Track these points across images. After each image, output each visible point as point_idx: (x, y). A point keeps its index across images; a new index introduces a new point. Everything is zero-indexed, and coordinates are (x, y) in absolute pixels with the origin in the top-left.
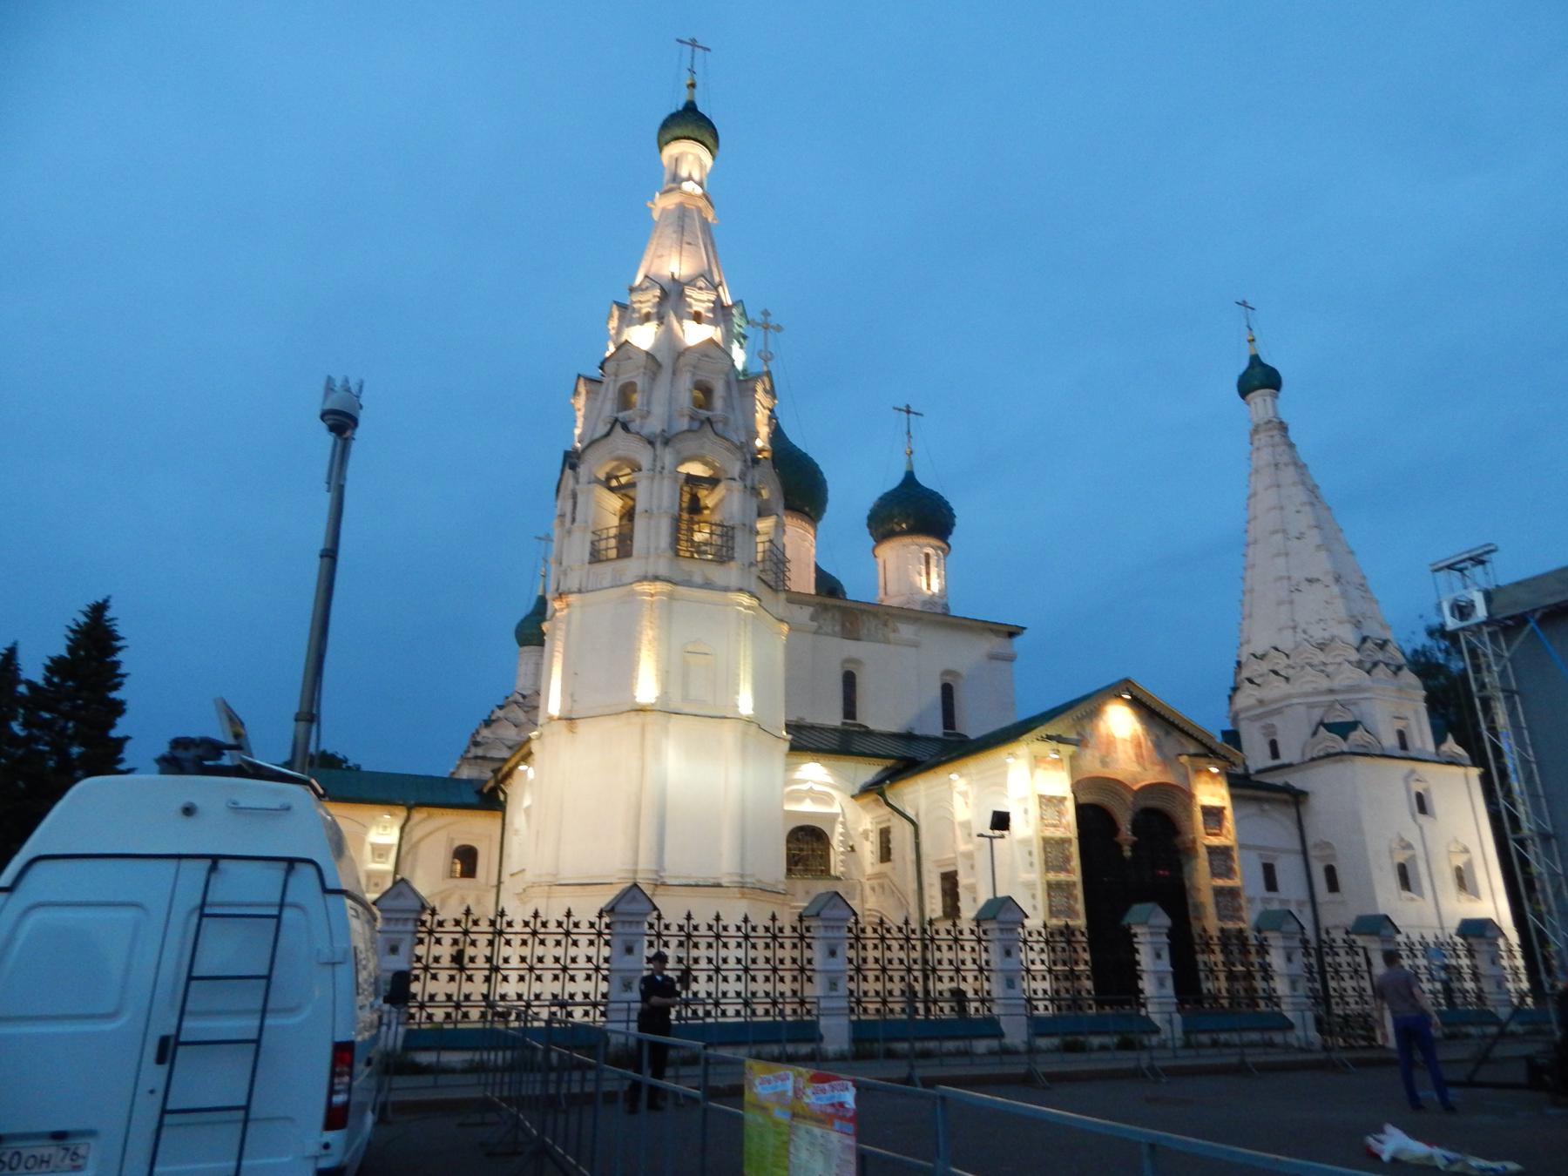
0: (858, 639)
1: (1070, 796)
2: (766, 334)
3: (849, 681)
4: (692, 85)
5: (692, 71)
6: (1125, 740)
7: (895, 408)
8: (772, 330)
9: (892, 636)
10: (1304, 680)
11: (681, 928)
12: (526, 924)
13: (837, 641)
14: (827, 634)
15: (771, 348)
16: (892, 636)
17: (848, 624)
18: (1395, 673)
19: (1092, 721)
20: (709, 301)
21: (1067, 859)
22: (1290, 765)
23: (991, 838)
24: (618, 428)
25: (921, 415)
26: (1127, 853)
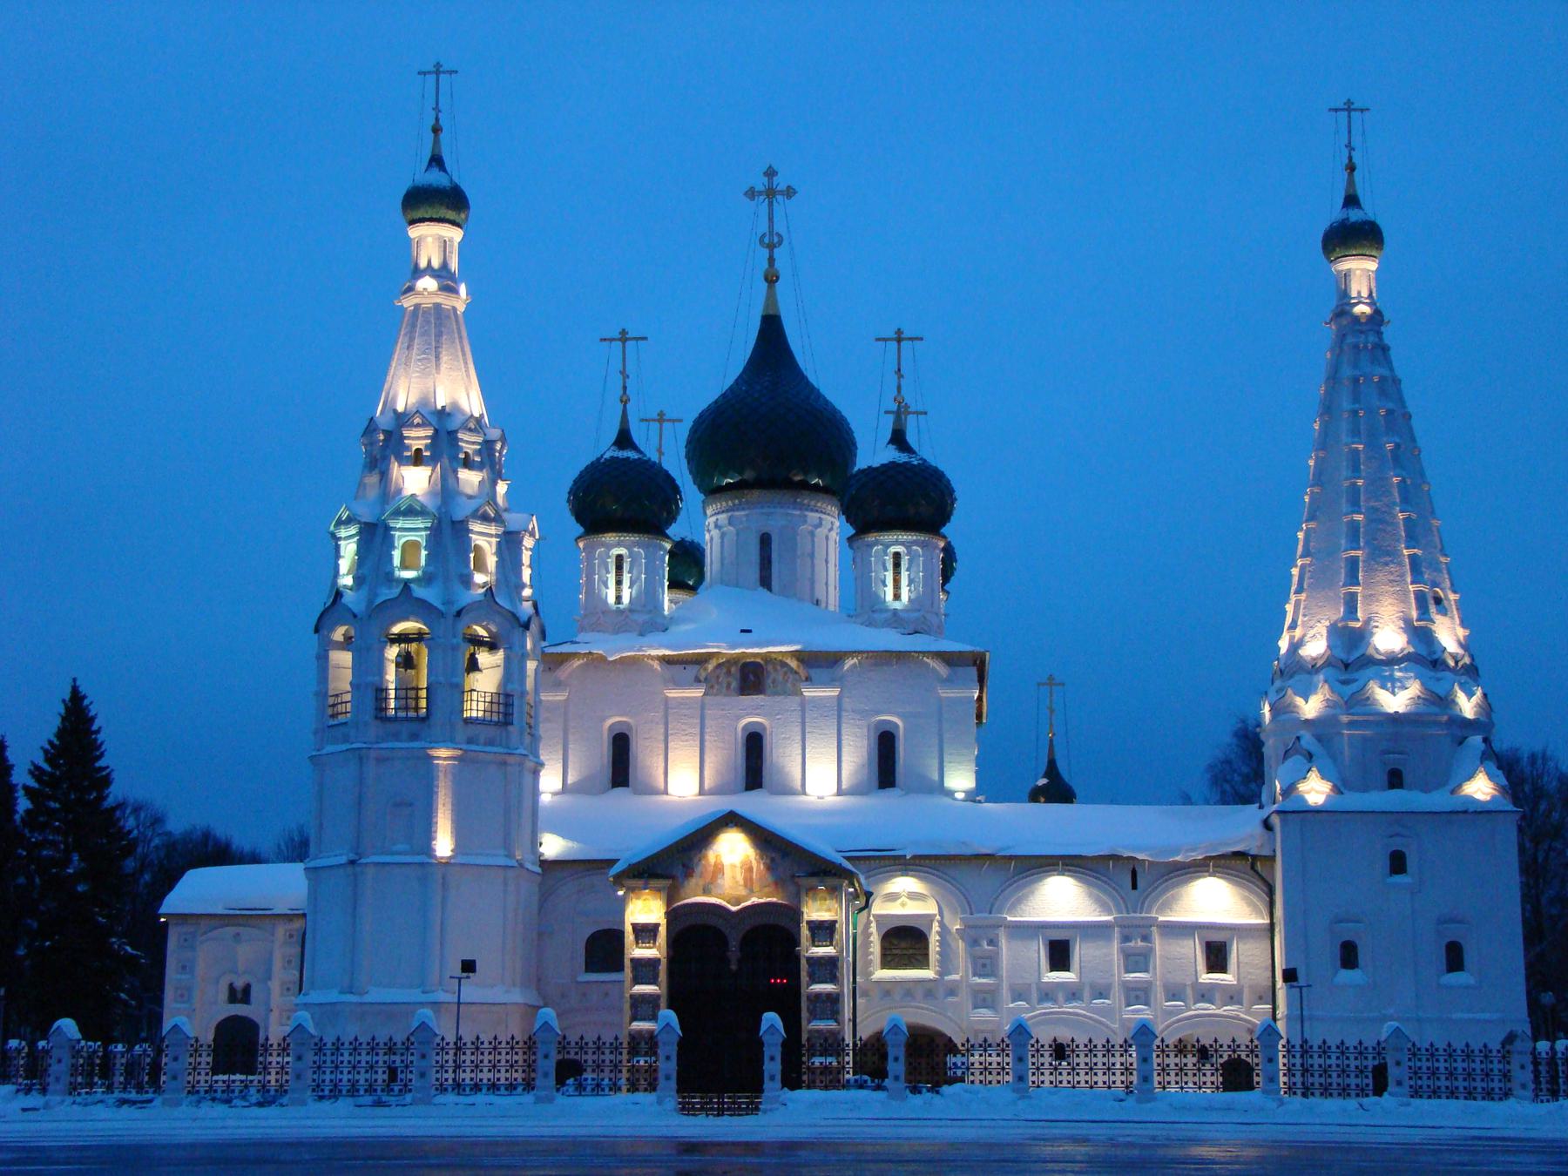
1: (663, 922)
2: (771, 204)
4: (436, 130)
5: (437, 109)
6: (734, 866)
7: (878, 340)
8: (779, 198)
15: (779, 227)
19: (701, 851)
20: (426, 437)
23: (460, 979)
25: (922, 339)
26: (734, 967)
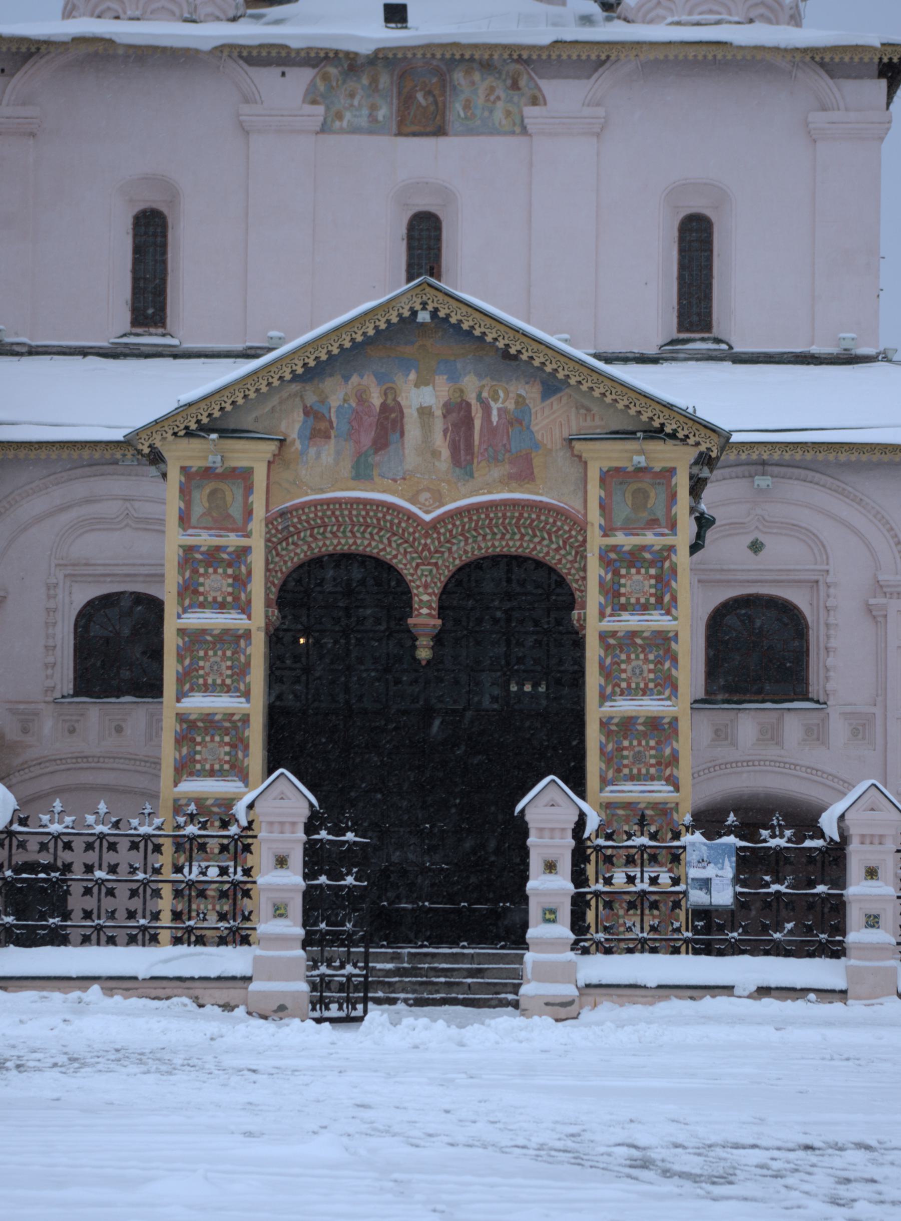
0: (440, 131)
6: (425, 412)
9: (530, 111)
13: (385, 141)
14: (355, 130)
17: (420, 96)
21: (242, 671)
26: (424, 654)
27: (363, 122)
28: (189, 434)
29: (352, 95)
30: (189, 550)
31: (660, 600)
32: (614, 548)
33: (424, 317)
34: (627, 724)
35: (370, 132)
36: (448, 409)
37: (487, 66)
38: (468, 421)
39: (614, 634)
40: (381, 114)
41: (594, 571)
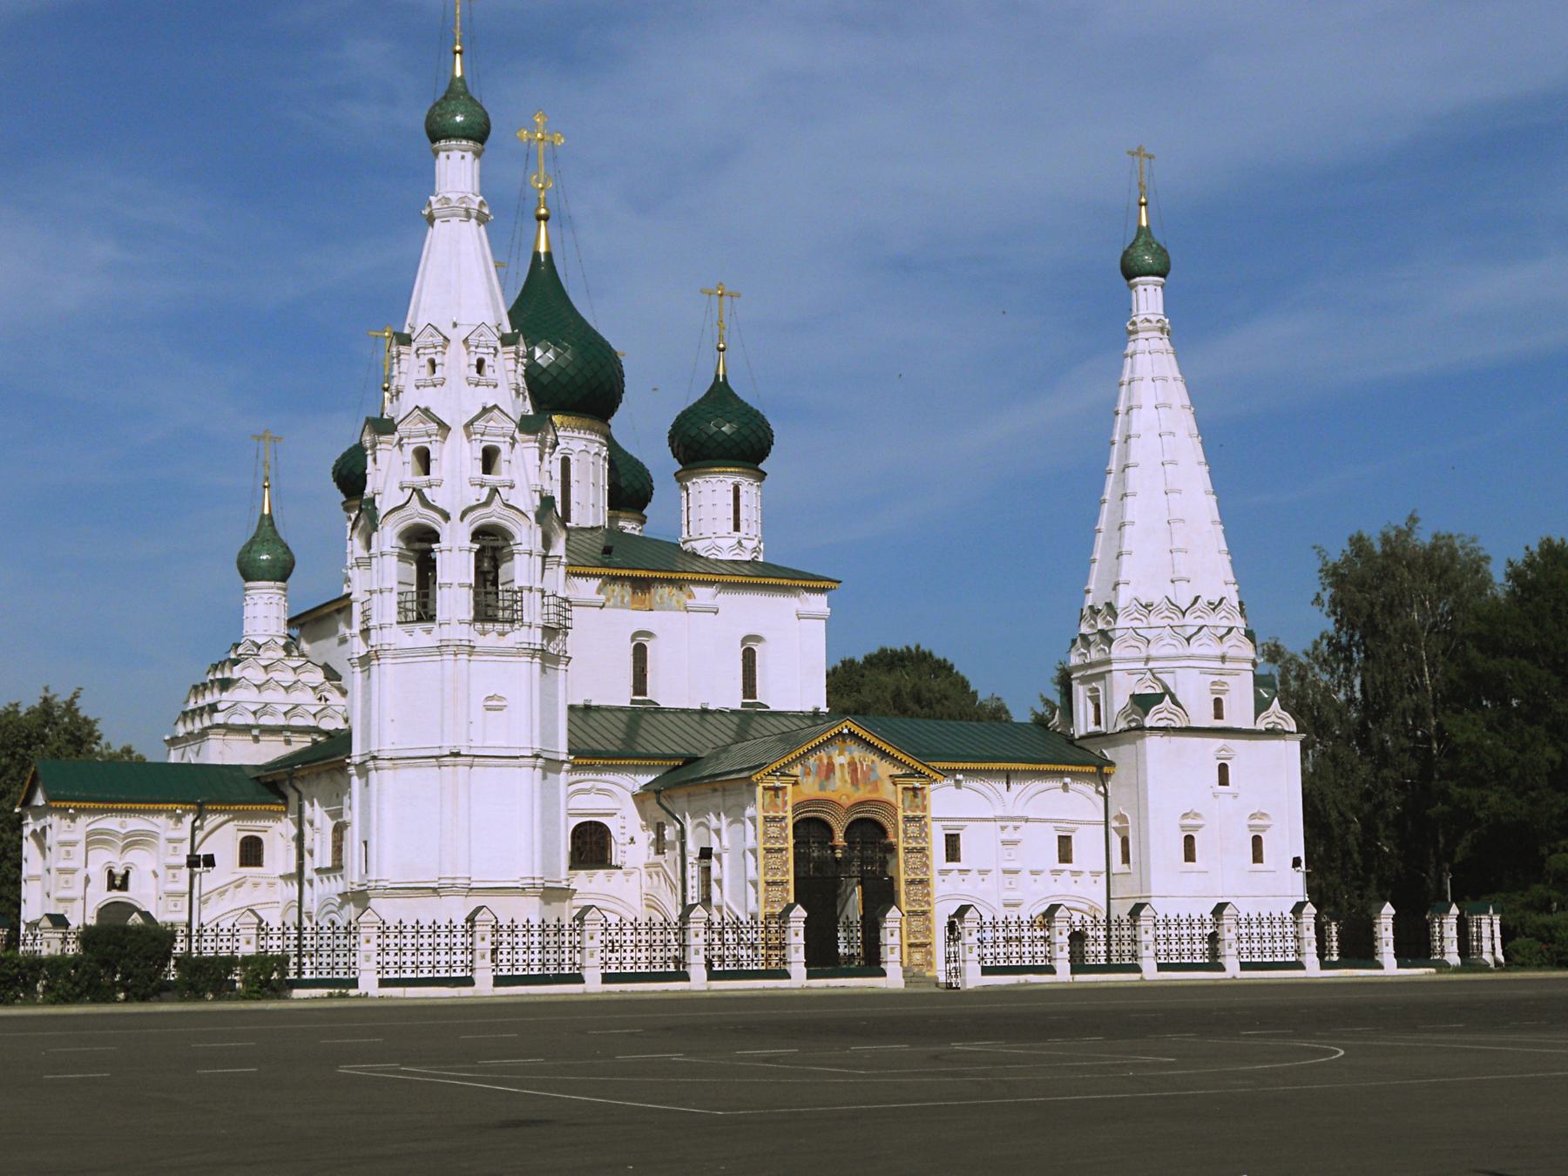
3: (640, 653)
6: (842, 765)
9: (690, 602)
10: (1126, 644)
11: (509, 927)
12: (430, 927)
14: (615, 606)
16: (690, 602)
18: (1221, 638)
21: (786, 862)
22: (1105, 734)
24: (415, 496)
27: (619, 604)
28: (769, 774)
29: (613, 591)
30: (765, 817)
31: (920, 834)
32: (905, 817)
33: (846, 731)
34: (912, 882)
35: (622, 607)
36: (849, 764)
37: (670, 582)
38: (856, 769)
39: (907, 848)
40: (627, 599)
41: (901, 826)
